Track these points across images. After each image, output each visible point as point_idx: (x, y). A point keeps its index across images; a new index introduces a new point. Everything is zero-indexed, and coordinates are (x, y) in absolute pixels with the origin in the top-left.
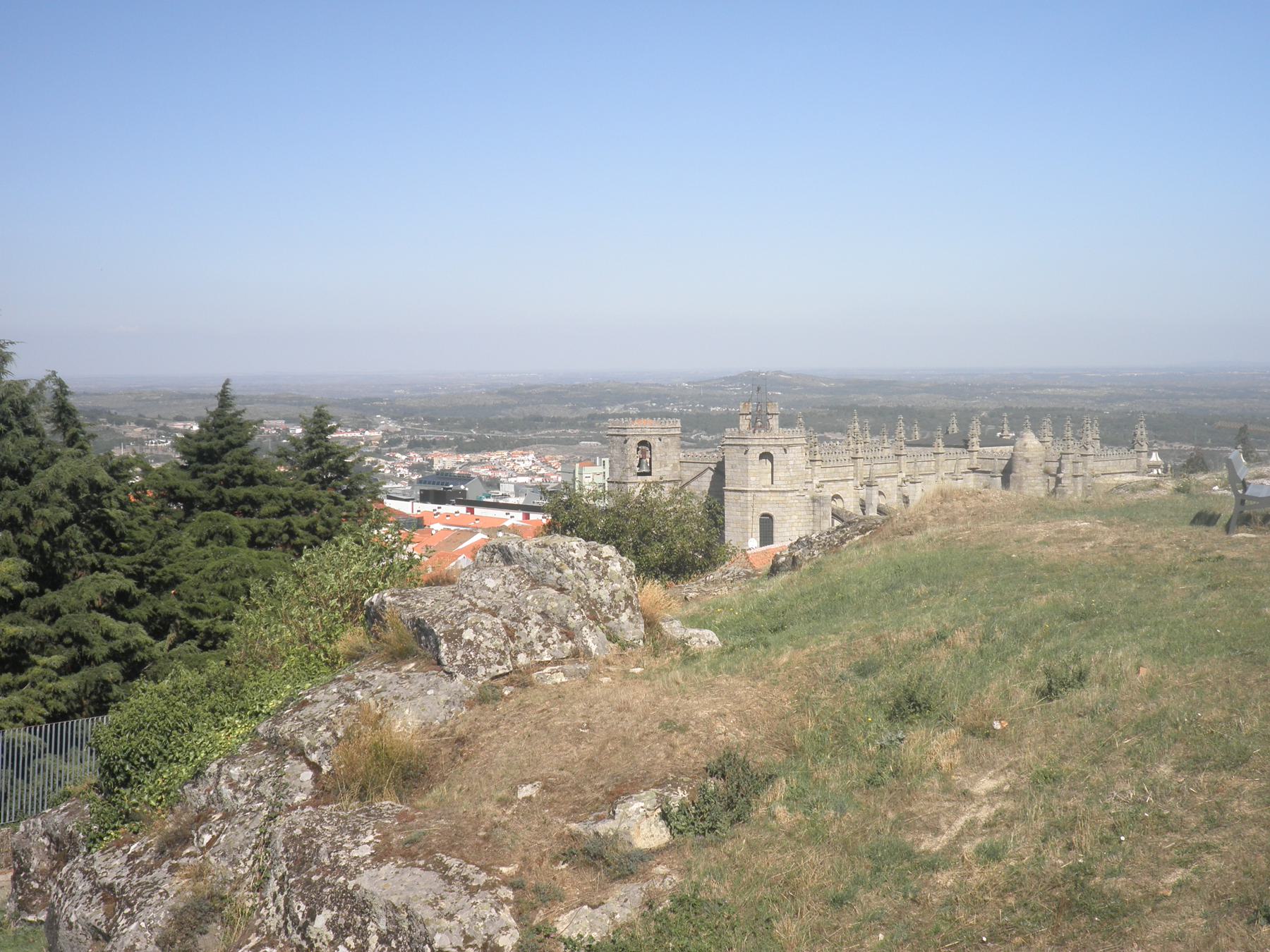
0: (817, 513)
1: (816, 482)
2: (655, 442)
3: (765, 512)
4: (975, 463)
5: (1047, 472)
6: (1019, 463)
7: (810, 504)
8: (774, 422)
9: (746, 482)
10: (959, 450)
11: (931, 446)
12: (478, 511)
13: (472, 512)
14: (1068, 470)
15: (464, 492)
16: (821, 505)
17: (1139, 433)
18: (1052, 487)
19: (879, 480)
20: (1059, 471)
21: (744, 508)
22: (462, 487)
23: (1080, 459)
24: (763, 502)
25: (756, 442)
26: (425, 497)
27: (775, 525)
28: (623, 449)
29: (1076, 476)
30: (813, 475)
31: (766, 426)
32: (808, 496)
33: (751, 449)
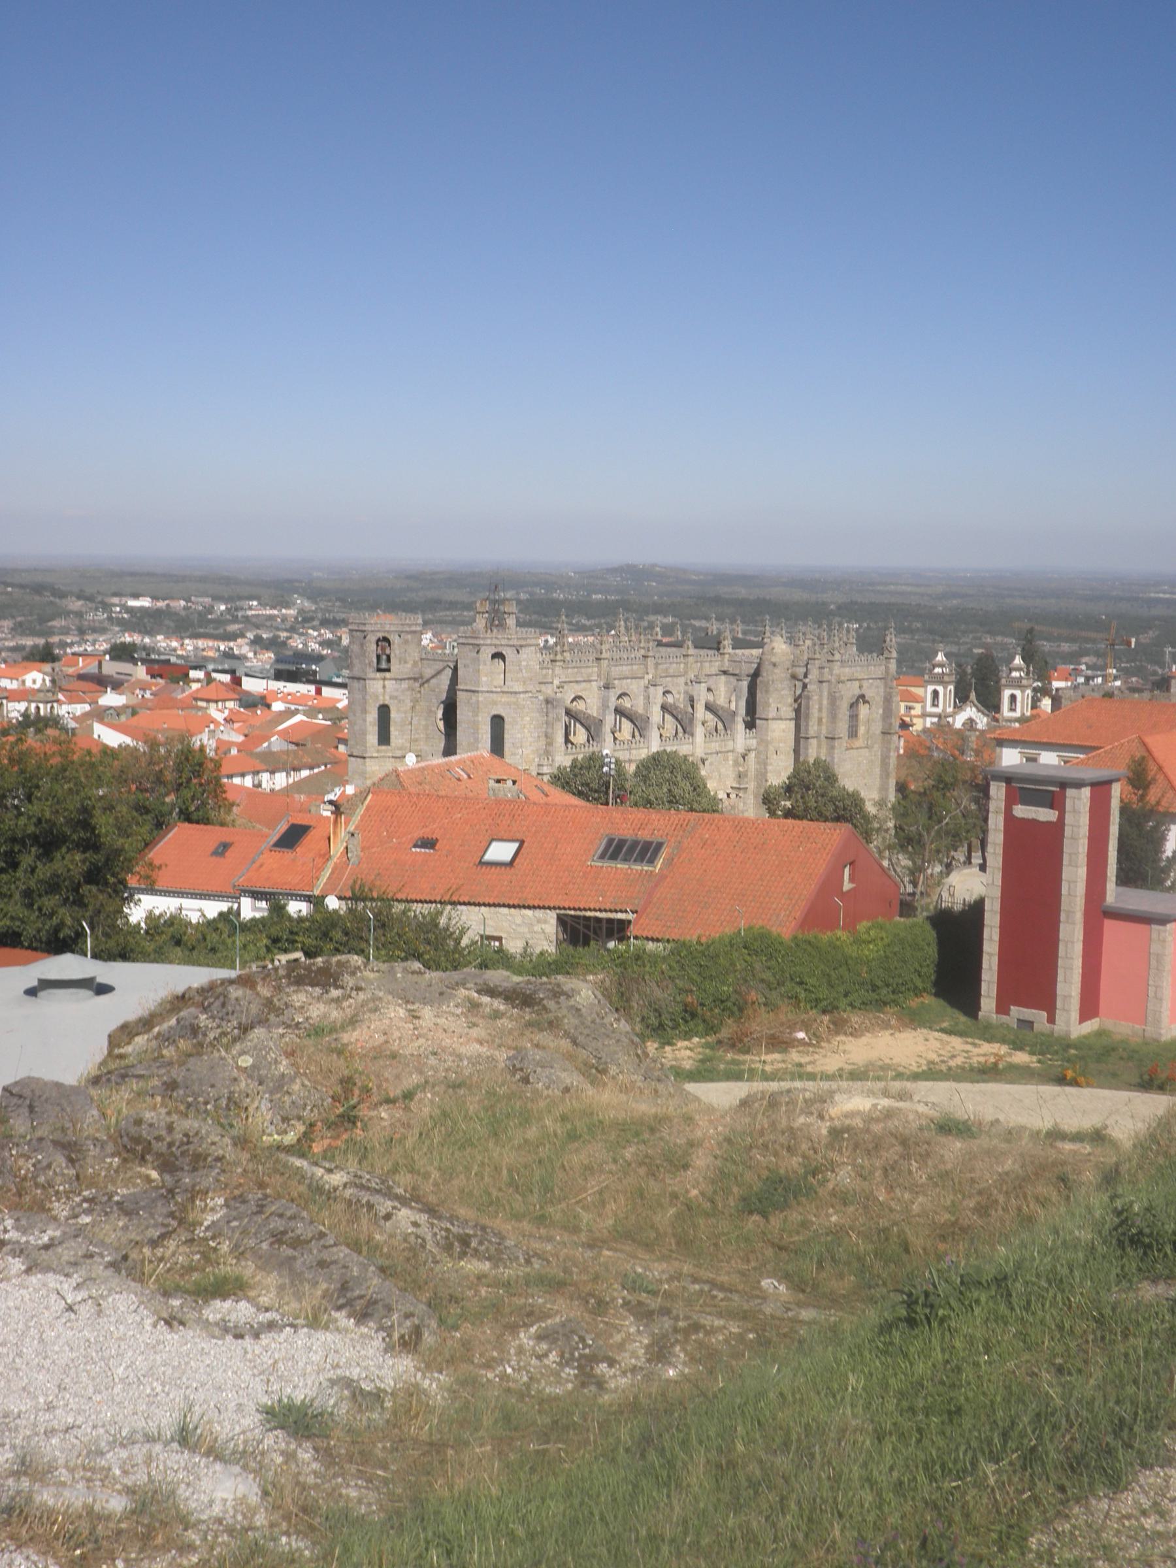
0: (550, 715)
1: (556, 682)
2: (394, 639)
3: (496, 713)
4: (726, 665)
5: (794, 677)
6: (766, 667)
7: (544, 706)
8: (511, 621)
9: (478, 682)
10: (711, 652)
11: (681, 646)
12: (327, 691)
13: (319, 692)
14: (814, 675)
15: (315, 672)
16: (554, 707)
17: (888, 639)
18: (798, 692)
19: (616, 682)
20: (806, 676)
21: (476, 709)
22: (314, 667)
23: (826, 664)
24: (495, 703)
25: (489, 642)
26: (279, 676)
27: (506, 726)
28: (362, 645)
29: (821, 682)
30: (554, 676)
31: (502, 626)
32: (541, 698)
33: (483, 649)
